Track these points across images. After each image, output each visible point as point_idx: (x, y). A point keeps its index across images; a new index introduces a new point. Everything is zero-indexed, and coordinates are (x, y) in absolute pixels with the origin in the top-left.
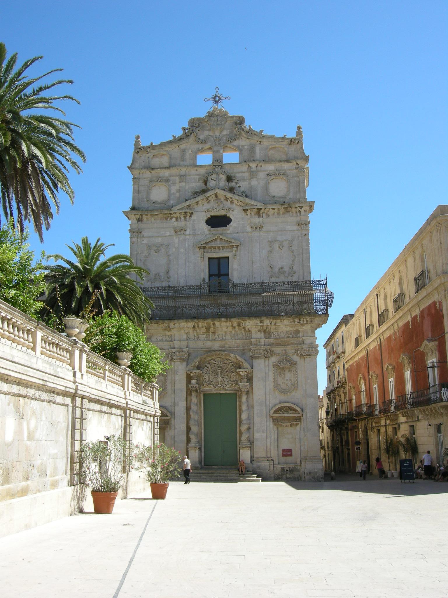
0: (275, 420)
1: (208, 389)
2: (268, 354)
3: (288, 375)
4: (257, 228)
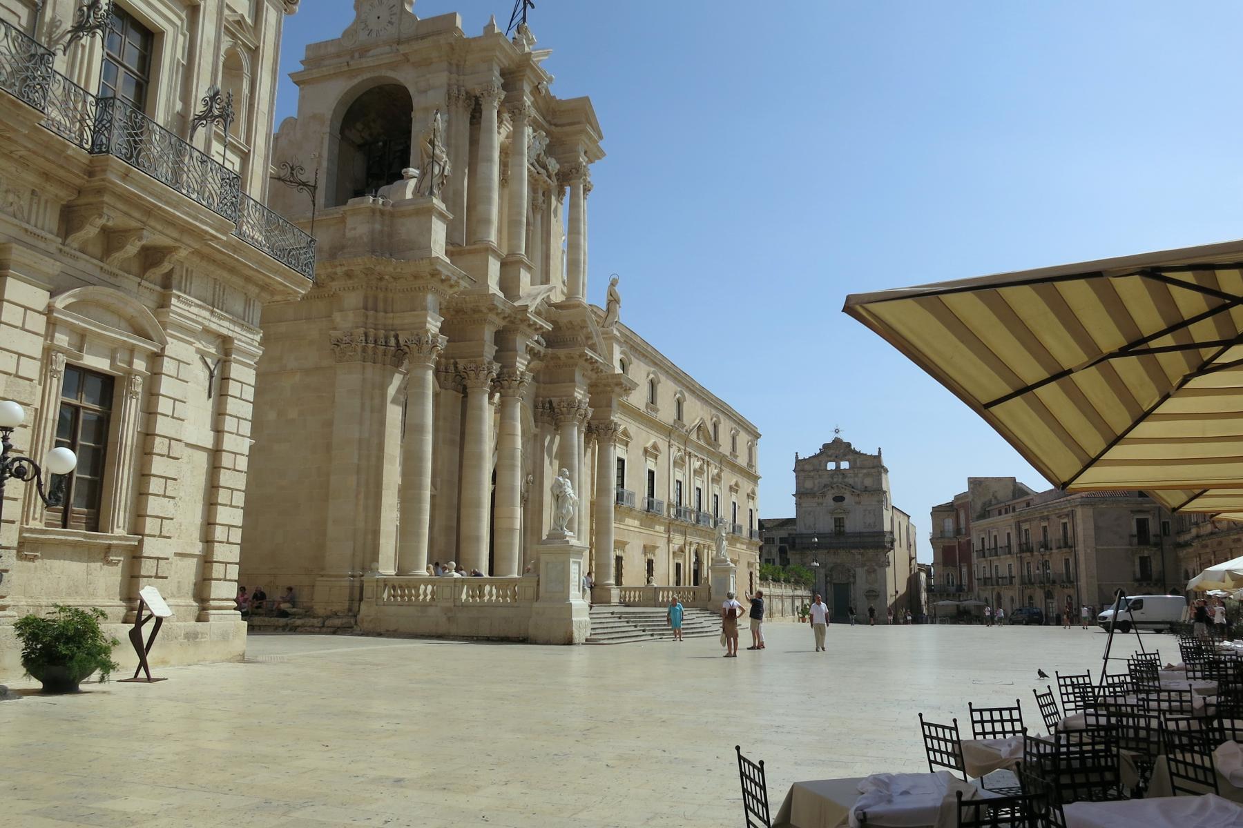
0: (866, 596)
1: (835, 581)
2: (863, 565)
3: (873, 575)
4: (859, 503)
